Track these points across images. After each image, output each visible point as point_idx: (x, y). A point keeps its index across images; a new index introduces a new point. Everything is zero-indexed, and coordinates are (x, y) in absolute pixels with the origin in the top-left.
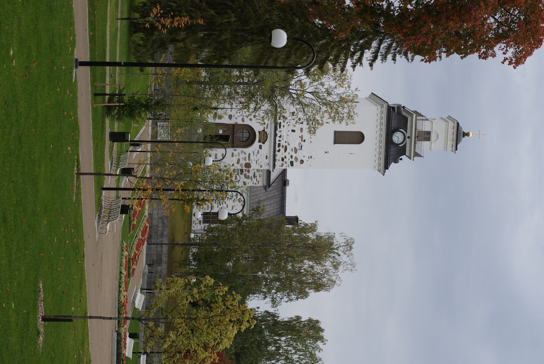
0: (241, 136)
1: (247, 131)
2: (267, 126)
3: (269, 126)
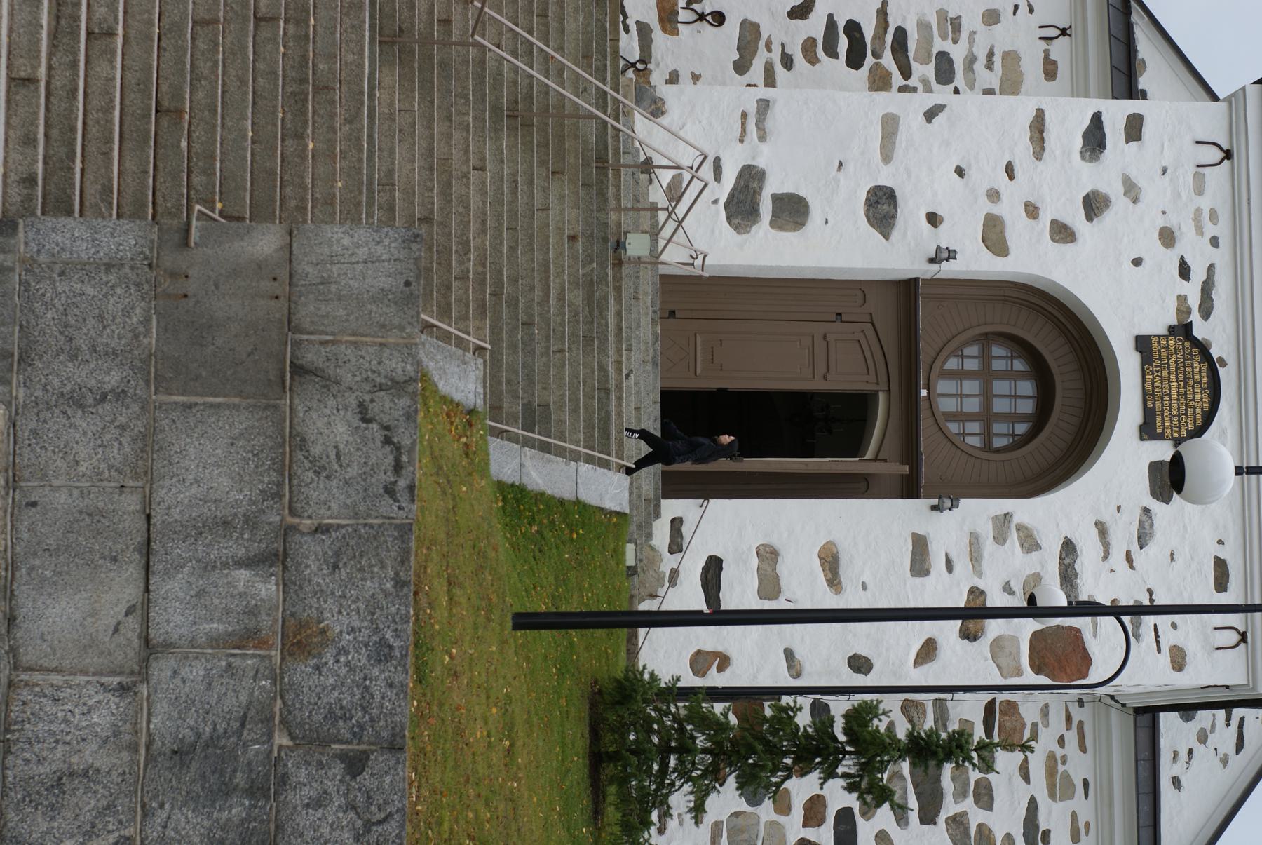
0: (972, 405)
1: (1019, 366)
2: (1207, 289)
3: (1222, 295)
